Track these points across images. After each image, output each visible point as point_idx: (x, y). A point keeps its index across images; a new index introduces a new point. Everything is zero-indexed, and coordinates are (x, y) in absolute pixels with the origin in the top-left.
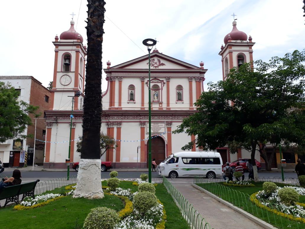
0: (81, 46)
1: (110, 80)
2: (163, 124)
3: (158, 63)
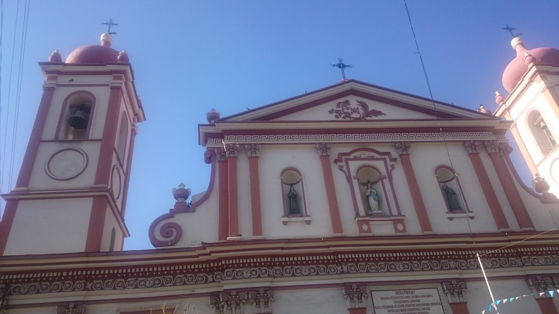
0: (127, 79)
1: (220, 156)
2: (434, 292)
3: (361, 111)
